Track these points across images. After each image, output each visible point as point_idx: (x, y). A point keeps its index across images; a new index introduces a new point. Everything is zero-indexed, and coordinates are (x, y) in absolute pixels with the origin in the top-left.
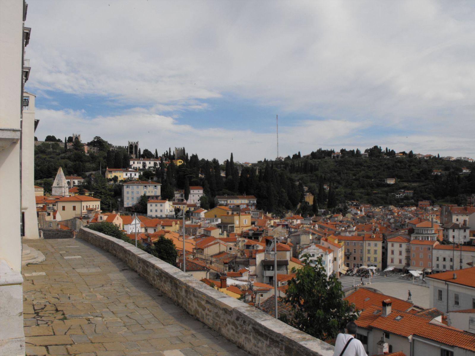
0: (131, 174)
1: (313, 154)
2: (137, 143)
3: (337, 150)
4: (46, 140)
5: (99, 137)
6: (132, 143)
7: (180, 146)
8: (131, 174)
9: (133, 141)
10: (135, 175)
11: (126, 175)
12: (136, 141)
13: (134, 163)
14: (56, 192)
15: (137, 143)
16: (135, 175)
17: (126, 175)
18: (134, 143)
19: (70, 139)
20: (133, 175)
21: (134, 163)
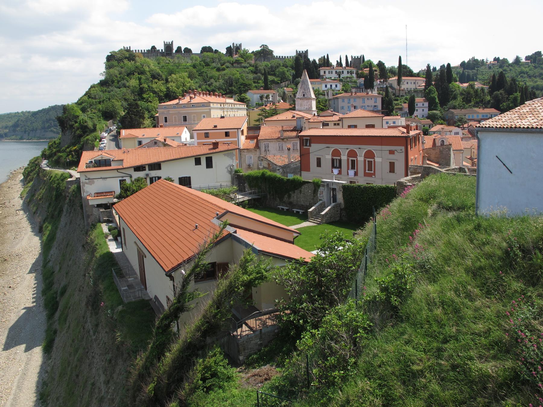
0: (331, 86)
1: (463, 64)
2: (307, 52)
3: (491, 59)
4: (202, 52)
5: (266, 45)
6: (300, 52)
7: (357, 54)
8: (331, 86)
9: (302, 49)
10: (336, 86)
11: (326, 86)
12: (304, 50)
13: (325, 72)
14: (301, 105)
15: (307, 52)
16: (336, 86)
17: (326, 86)
18: (303, 52)
19: (229, 50)
20: (334, 86)
21: (325, 72)
